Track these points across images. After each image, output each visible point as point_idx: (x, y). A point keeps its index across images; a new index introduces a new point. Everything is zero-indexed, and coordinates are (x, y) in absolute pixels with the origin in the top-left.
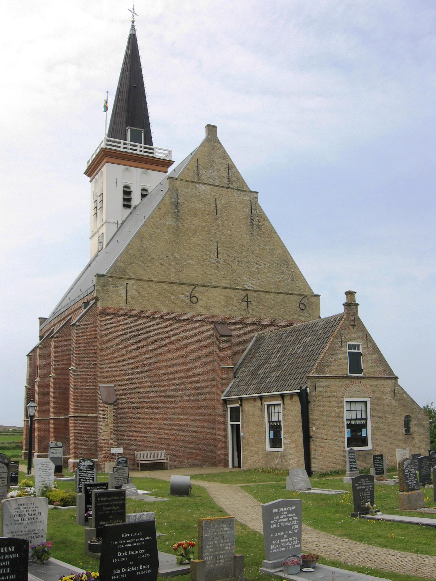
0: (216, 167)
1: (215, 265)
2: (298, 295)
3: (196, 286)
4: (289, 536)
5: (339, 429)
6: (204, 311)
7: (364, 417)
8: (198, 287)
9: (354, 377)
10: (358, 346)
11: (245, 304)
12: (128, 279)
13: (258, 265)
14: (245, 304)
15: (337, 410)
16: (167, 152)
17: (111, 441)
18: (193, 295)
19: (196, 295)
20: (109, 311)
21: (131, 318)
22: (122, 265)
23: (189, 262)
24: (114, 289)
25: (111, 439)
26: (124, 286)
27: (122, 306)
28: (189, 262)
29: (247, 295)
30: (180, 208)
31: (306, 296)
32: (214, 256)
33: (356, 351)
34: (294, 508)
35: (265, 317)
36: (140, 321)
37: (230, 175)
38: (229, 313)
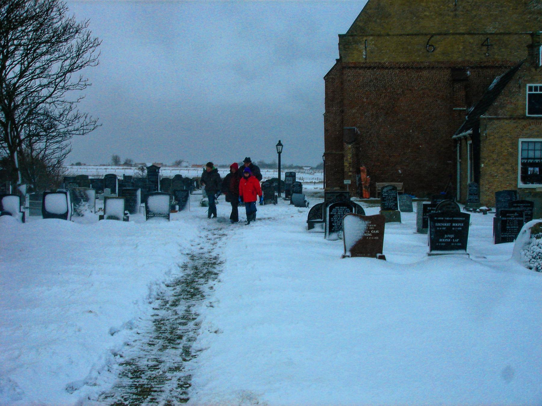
1: (452, 14)
8: (435, 37)
9: (533, 118)
11: (485, 48)
12: (366, 36)
15: (510, 150)
17: (350, 174)
20: (351, 65)
21: (371, 70)
22: (361, 24)
24: (354, 46)
25: (350, 172)
35: (508, 59)
36: (378, 72)
38: (467, 58)
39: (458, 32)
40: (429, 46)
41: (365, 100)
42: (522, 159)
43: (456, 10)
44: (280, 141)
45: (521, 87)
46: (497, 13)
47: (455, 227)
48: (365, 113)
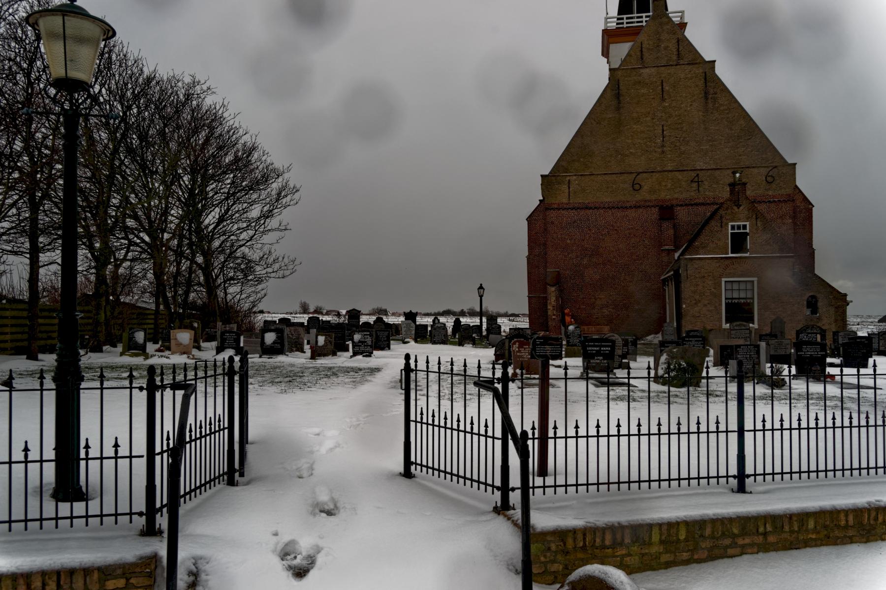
0: (663, 45)
2: (765, 167)
3: (639, 173)
4: (365, 346)
5: (716, 307)
6: (648, 197)
7: (749, 295)
8: (641, 175)
10: (745, 227)
11: (695, 185)
13: (714, 141)
14: (695, 185)
15: (713, 289)
16: (680, 14)
17: (554, 317)
18: (635, 182)
19: (639, 182)
21: (574, 211)
23: (631, 150)
25: (554, 315)
26: (566, 183)
27: (565, 201)
28: (631, 150)
29: (698, 175)
30: (621, 98)
31: (776, 167)
32: (659, 141)
33: (742, 231)
34: (368, 333)
36: (582, 212)
37: (680, 50)
38: (676, 196)
39: (666, 169)
40: (636, 187)
41: (569, 241)
42: (726, 299)
43: (663, 146)
44: (481, 285)
45: (723, 225)
46: (708, 147)
47: (603, 350)
48: (568, 255)
